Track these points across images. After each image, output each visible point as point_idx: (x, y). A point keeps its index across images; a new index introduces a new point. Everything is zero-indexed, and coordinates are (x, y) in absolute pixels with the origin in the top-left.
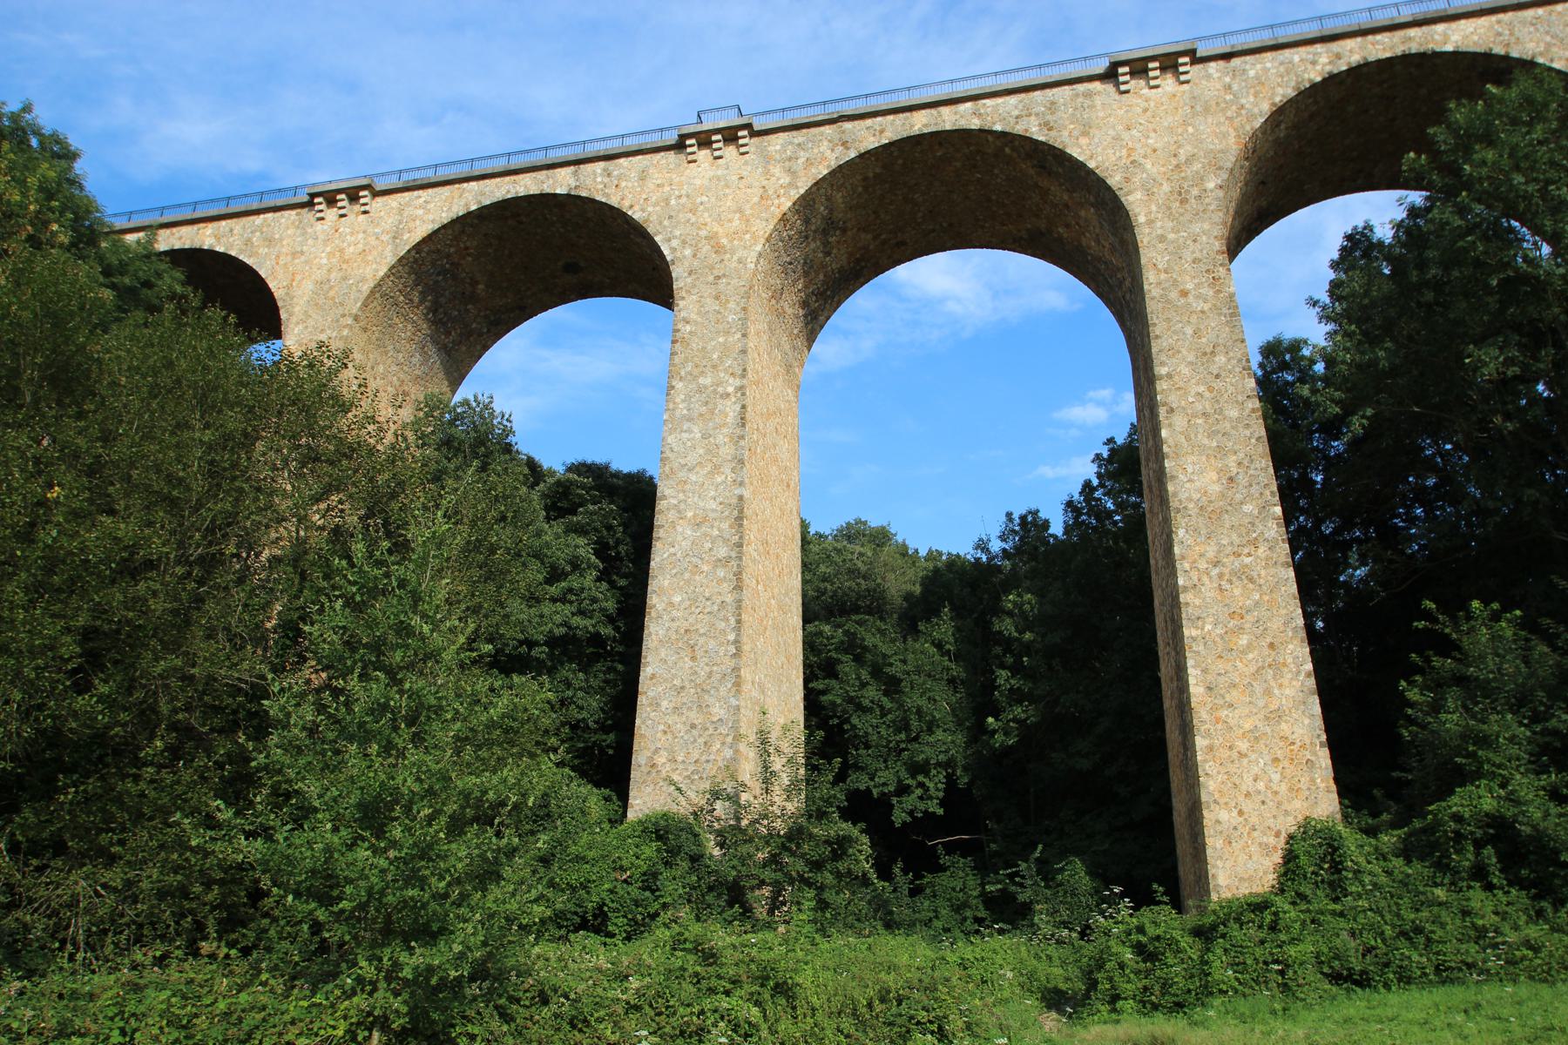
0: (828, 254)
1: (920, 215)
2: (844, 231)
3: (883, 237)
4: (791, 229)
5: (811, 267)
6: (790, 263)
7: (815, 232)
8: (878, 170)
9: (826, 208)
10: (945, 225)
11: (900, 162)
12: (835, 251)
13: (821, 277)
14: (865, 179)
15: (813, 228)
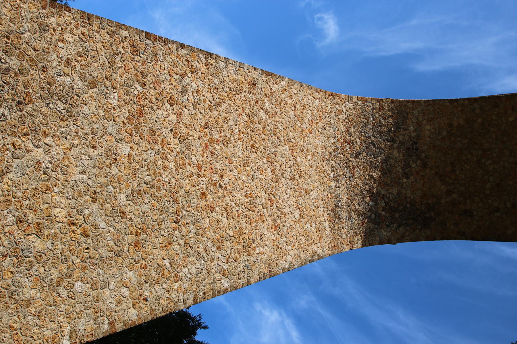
0: (406, 175)
1: (489, 185)
2: (424, 166)
3: (455, 196)
4: (384, 119)
5: (389, 171)
6: (374, 146)
7: (402, 143)
8: (461, 122)
9: (415, 130)
10: (508, 204)
11: (480, 120)
12: (412, 179)
13: (395, 191)
14: (450, 125)
15: (401, 137)
